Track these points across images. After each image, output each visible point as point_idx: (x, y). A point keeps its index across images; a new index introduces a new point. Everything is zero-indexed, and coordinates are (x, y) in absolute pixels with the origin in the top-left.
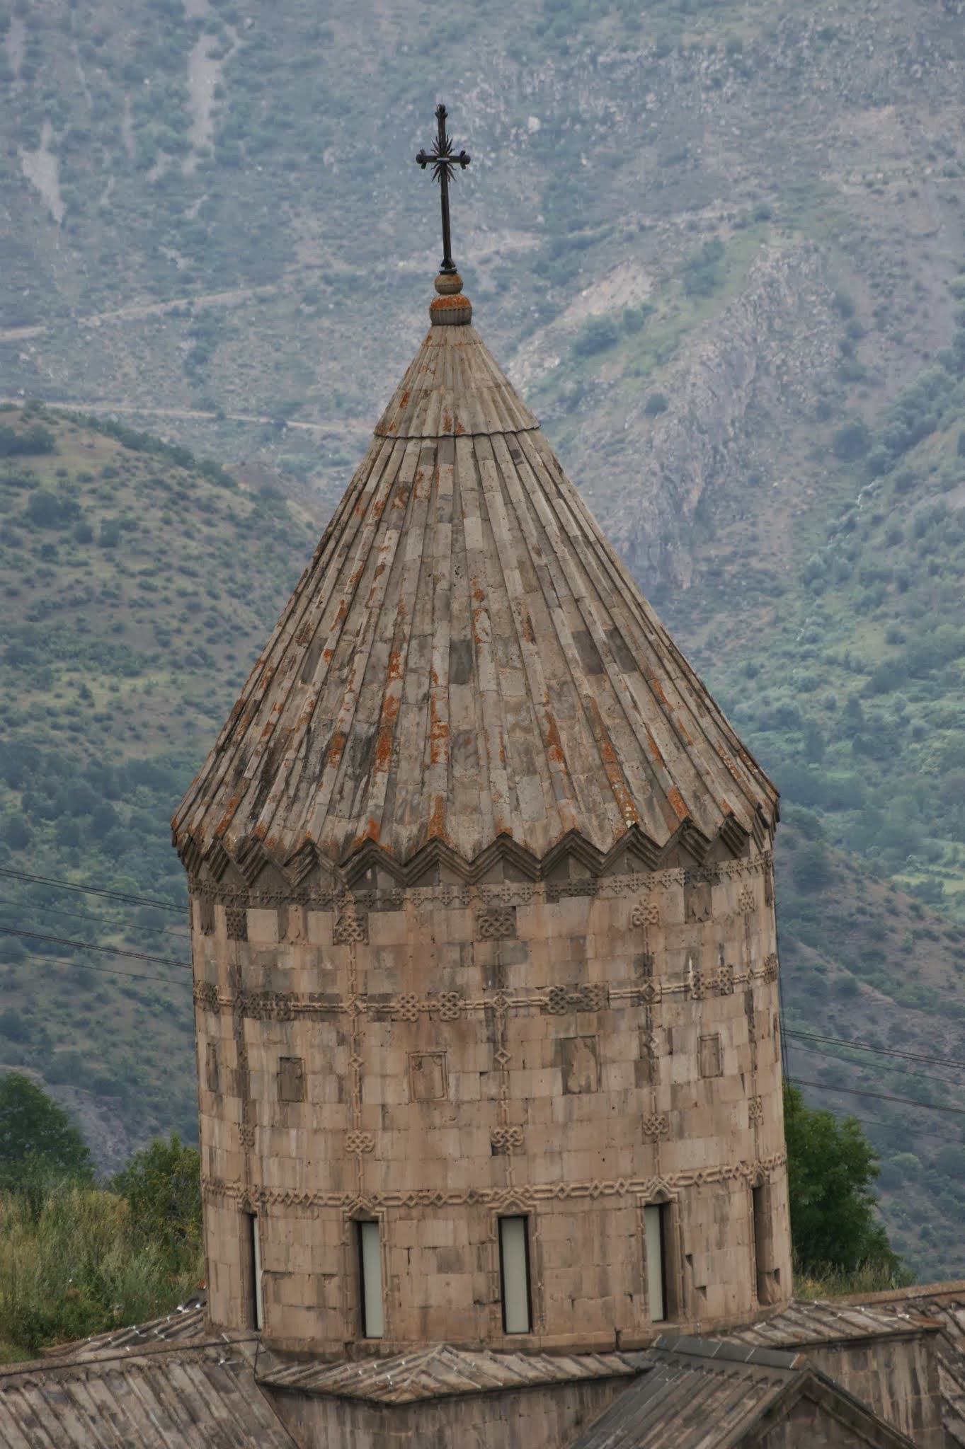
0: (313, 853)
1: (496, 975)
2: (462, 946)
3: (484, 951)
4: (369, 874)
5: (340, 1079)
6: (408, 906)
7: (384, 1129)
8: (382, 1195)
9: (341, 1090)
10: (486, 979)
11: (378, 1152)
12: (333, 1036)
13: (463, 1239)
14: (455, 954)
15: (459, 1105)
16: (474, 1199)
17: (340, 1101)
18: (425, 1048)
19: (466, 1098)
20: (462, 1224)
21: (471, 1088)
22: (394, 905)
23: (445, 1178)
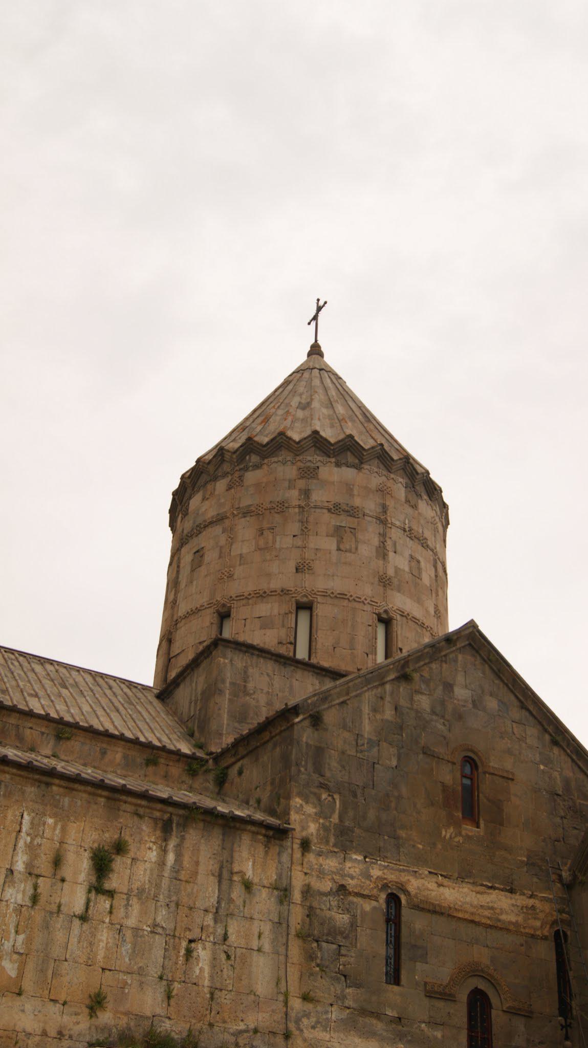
0: (222, 455)
1: (306, 493)
2: (290, 481)
3: (301, 484)
4: (247, 458)
5: (221, 547)
6: (265, 467)
7: (240, 565)
8: (234, 596)
9: (221, 552)
10: (300, 495)
11: (235, 577)
12: (221, 530)
13: (276, 611)
14: (286, 484)
15: (281, 549)
16: (284, 592)
17: (220, 557)
18: (265, 525)
19: (285, 546)
20: (276, 605)
21: (288, 542)
22: (257, 467)
23: (269, 583)
